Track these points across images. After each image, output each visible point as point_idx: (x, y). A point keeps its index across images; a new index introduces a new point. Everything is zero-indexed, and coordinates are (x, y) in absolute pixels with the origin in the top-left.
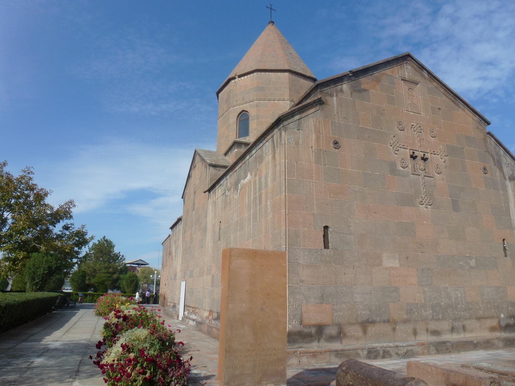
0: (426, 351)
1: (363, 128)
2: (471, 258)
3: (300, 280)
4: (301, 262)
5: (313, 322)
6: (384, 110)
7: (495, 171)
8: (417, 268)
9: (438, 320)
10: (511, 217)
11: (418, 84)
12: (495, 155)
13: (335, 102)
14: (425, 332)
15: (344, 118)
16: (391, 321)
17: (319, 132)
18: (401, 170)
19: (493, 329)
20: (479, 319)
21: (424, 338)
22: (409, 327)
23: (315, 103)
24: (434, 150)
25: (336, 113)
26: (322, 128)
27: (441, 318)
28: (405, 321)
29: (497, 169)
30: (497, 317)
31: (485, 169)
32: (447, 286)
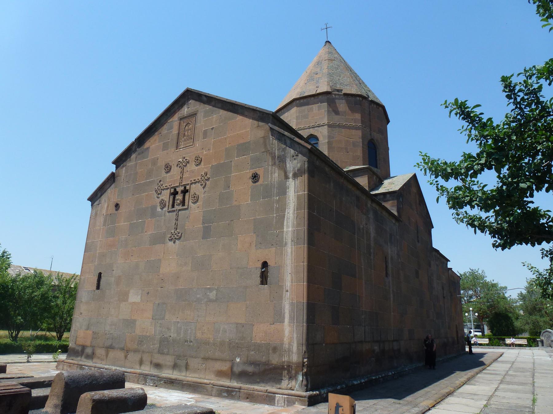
0: (136, 380)
1: (138, 184)
2: (210, 290)
4: (83, 300)
5: (81, 343)
6: (158, 159)
7: (271, 173)
9: (163, 354)
10: (283, 229)
11: (196, 114)
12: (276, 151)
13: (124, 172)
14: (149, 363)
15: (127, 182)
16: (125, 349)
17: (110, 201)
18: (159, 211)
19: (220, 374)
20: (206, 359)
21: (147, 369)
22: (137, 357)
23: (109, 179)
24: (194, 179)
25: (122, 181)
26: (112, 197)
28: (136, 351)
29: (276, 169)
30: (230, 361)
31: (255, 177)
32: (178, 321)
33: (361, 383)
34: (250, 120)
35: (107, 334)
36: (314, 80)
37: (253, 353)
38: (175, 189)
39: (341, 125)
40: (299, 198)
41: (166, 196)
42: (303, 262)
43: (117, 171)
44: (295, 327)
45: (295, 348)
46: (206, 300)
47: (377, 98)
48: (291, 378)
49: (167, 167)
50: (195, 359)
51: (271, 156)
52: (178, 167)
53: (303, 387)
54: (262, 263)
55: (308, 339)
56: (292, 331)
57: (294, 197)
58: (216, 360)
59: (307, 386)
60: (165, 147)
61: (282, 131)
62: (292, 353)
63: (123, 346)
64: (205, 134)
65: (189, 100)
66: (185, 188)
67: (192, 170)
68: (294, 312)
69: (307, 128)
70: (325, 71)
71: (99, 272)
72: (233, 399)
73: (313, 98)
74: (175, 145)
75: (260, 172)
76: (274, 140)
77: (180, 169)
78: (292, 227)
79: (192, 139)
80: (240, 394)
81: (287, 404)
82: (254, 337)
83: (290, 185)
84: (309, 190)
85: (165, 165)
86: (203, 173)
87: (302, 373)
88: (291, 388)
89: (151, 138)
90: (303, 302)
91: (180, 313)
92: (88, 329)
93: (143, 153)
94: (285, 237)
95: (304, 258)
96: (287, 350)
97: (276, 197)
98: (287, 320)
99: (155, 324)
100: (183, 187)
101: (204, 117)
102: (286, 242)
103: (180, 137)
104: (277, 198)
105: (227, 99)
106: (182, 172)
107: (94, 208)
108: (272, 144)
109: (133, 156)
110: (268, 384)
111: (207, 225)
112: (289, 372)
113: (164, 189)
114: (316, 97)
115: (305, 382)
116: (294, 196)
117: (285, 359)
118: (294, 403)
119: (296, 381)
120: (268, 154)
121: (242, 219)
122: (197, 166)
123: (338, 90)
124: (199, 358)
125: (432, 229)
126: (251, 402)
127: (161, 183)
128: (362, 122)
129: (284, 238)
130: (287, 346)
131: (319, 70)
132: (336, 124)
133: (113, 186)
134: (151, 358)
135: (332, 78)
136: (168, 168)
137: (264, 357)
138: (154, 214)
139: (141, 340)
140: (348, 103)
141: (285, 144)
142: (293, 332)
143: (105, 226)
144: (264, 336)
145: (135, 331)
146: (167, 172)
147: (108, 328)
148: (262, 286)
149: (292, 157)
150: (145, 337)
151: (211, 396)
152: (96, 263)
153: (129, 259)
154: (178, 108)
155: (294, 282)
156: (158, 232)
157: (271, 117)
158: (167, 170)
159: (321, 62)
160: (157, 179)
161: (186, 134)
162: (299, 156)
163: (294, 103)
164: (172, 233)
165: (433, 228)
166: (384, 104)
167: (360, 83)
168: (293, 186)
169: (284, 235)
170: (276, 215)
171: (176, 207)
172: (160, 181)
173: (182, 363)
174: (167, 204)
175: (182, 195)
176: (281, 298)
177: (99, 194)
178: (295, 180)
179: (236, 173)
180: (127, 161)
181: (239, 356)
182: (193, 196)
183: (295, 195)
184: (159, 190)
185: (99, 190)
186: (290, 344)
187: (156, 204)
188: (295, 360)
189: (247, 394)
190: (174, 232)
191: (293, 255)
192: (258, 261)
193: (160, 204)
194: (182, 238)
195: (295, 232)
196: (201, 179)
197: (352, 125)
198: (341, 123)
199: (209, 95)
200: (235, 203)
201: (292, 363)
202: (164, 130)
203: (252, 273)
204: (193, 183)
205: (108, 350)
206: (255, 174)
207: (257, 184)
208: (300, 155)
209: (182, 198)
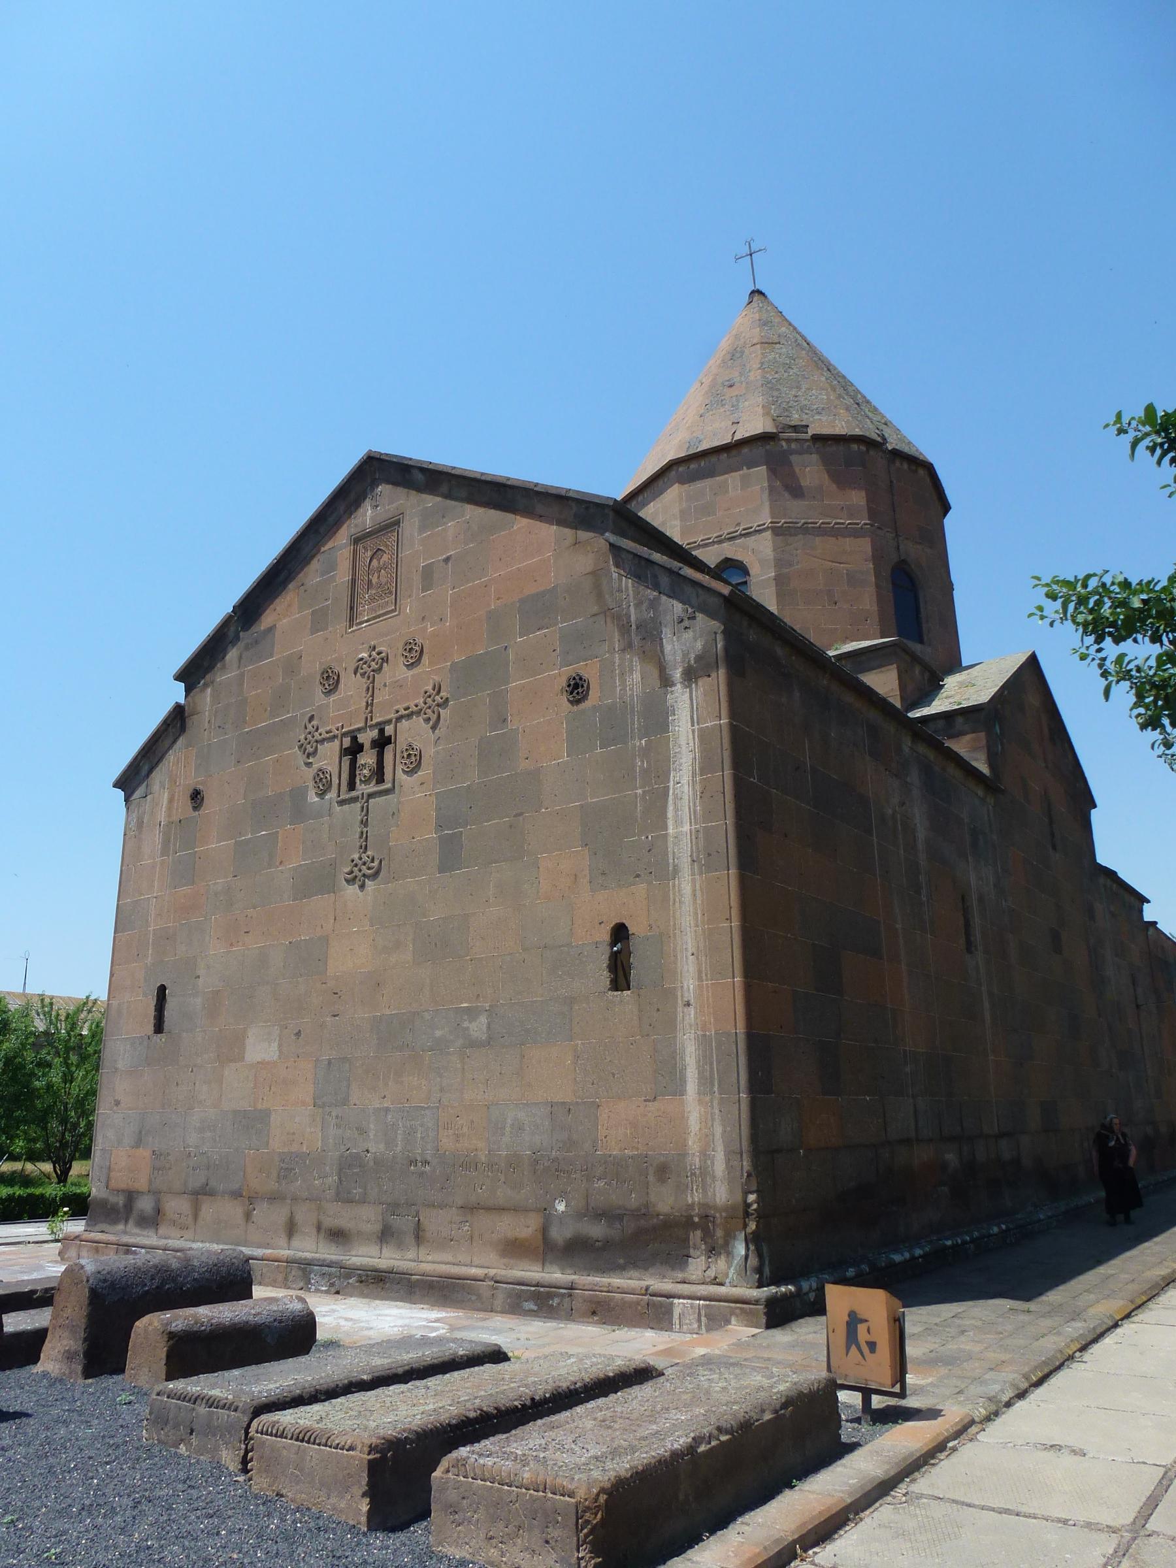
0: (280, 1278)
1: (251, 731)
2: (472, 1013)
3: (115, 1101)
4: (120, 1065)
5: (123, 1186)
7: (622, 674)
8: (317, 1060)
10: (666, 828)
11: (397, 523)
12: (632, 609)
13: (208, 699)
14: (314, 1231)
15: (219, 727)
19: (514, 1248)
20: (470, 1209)
21: (308, 1247)
22: (279, 1214)
23: (169, 725)
24: (405, 705)
25: (206, 725)
27: (357, 1198)
28: (274, 1198)
29: (635, 659)
30: (537, 1210)
31: (576, 686)
33: (913, 1258)
34: (552, 527)
35: (192, 1155)
36: (724, 402)
37: (601, 1184)
38: (354, 739)
39: (810, 525)
40: (704, 737)
41: (329, 758)
42: (727, 919)
43: (189, 698)
44: (715, 1103)
45: (719, 1166)
46: (460, 1042)
47: (910, 443)
48: (712, 1251)
49: (328, 677)
50: (441, 1211)
51: (618, 625)
52: (358, 674)
53: (748, 1273)
54: (613, 928)
55: (754, 1138)
56: (709, 1117)
57: (691, 736)
58: (502, 1209)
59: (759, 1270)
60: (319, 621)
61: (644, 551)
62: (714, 1178)
63: (237, 1186)
64: (428, 577)
65: (374, 484)
66: (382, 731)
67: (399, 680)
68: (711, 1064)
69: (713, 542)
70: (755, 375)
71: (159, 985)
72: (555, 1319)
73: (724, 456)
74: (345, 613)
75: (590, 671)
76: (624, 578)
77: (365, 680)
78: (691, 823)
79: (391, 593)
80: (574, 1302)
81: (706, 1326)
82: (601, 1140)
83: (676, 702)
84: (733, 714)
85: (323, 673)
86: (429, 688)
87: (743, 1233)
88: (716, 1278)
89: (277, 601)
90: (736, 1033)
91: (390, 1084)
92: (138, 1143)
93: (257, 642)
94: (674, 852)
95: (731, 908)
96: (698, 1172)
97: (641, 740)
98: (691, 1087)
99: (323, 1118)
100: (377, 731)
101: (422, 529)
102: (675, 866)
103: (359, 589)
104: (643, 742)
105: (483, 474)
106: (371, 689)
107: (132, 807)
108: (620, 590)
109: (232, 655)
110: (651, 1270)
111: (451, 832)
112: (707, 1234)
113: (323, 740)
114: (734, 452)
115: (753, 1261)
116: (690, 731)
117: (695, 1197)
118: (728, 1322)
119: (728, 1256)
120: (609, 620)
121: (547, 809)
122: (410, 667)
123: (795, 428)
124: (451, 1207)
125: (1093, 811)
126: (604, 1323)
127: (314, 723)
128: (872, 514)
129: (671, 856)
130: (698, 1160)
131: (737, 374)
132: (796, 525)
133: (181, 741)
134: (319, 1215)
135: (775, 393)
136: (331, 681)
137: (633, 1196)
138: (299, 811)
139: (288, 1166)
140: (827, 461)
141: (656, 587)
142: (713, 1120)
143: (168, 856)
144: (631, 1134)
145: (268, 1143)
146: (329, 693)
147: (193, 1138)
148: (616, 993)
149: (678, 623)
150: (297, 1157)
151: (492, 1311)
152: (150, 958)
153: (240, 944)
154: (345, 512)
155: (704, 978)
156: (317, 862)
157: (611, 514)
158: (327, 686)
159: (742, 352)
160: (303, 715)
161: (375, 580)
162: (698, 619)
163: (673, 473)
164: (353, 861)
165: (1095, 806)
166: (931, 457)
167: (858, 404)
168: (687, 705)
169: (670, 845)
170: (644, 792)
171: (361, 788)
172: (311, 718)
173: (404, 1223)
174: (335, 781)
175: (375, 751)
176: (671, 1024)
177: (146, 768)
178: (690, 687)
179: (522, 678)
180: (216, 669)
181: (563, 1195)
182: (405, 755)
183: (693, 731)
184: (309, 743)
185: (144, 756)
186: (704, 1154)
187: (304, 783)
188: (724, 1200)
189: (590, 1300)
190: (360, 859)
191: (699, 902)
192: (600, 923)
193: (316, 782)
194: (382, 874)
195: (701, 835)
196: (425, 703)
197: (843, 524)
198: (810, 521)
199: (430, 467)
200: (523, 765)
201: (715, 1208)
202: (312, 574)
203: (584, 959)
204: (402, 717)
205: (197, 1199)
206: (574, 679)
207: (582, 706)
208: (700, 616)
209: (375, 762)
